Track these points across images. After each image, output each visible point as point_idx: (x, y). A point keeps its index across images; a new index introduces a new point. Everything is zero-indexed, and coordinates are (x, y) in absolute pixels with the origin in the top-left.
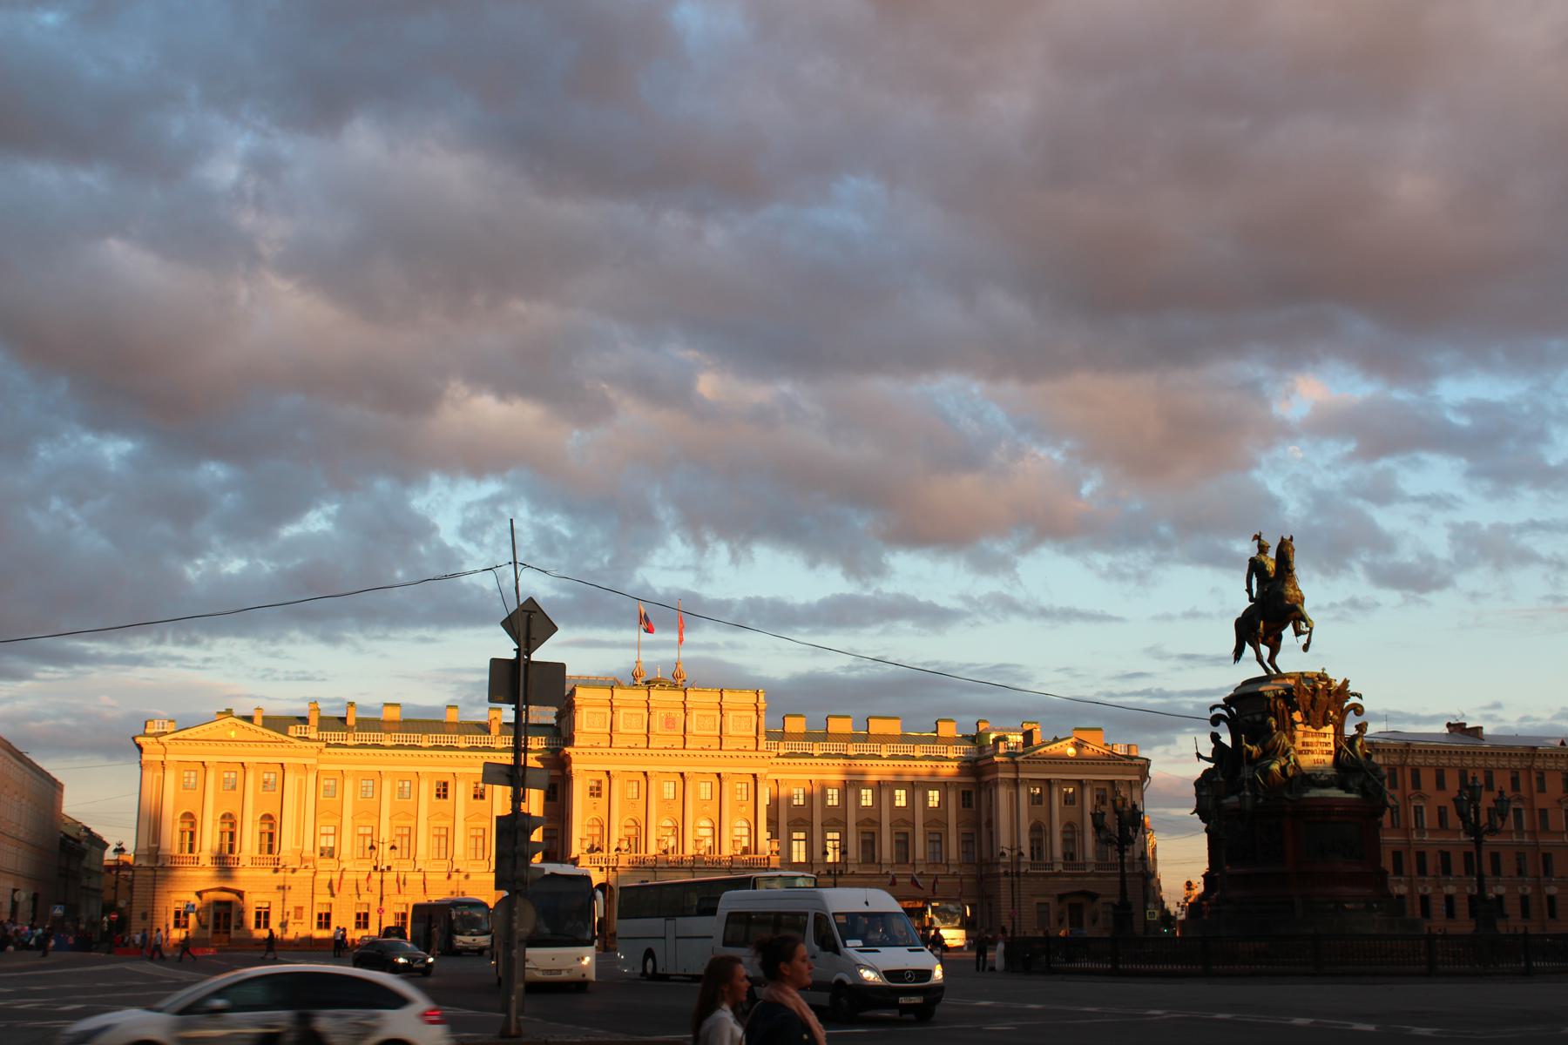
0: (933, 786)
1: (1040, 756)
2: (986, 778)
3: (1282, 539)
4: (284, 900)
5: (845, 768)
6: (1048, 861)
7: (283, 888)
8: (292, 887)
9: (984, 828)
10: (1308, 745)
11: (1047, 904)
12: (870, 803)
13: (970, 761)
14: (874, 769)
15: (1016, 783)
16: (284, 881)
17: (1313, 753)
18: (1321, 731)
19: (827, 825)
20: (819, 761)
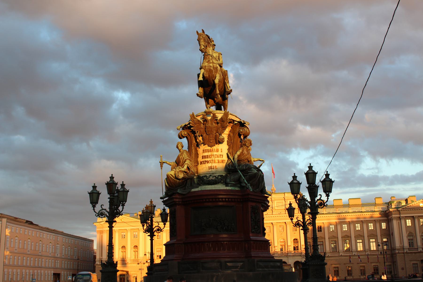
0: (370, 222)
1: (408, 208)
2: (390, 217)
3: (197, 32)
4: (141, 273)
5: (338, 217)
6: (416, 247)
7: (141, 269)
8: (144, 269)
9: (391, 235)
10: (205, 158)
11: (417, 264)
12: (346, 229)
13: (383, 212)
14: (349, 217)
15: (400, 218)
16: (141, 267)
17: (208, 162)
19: (330, 239)
20: (326, 215)
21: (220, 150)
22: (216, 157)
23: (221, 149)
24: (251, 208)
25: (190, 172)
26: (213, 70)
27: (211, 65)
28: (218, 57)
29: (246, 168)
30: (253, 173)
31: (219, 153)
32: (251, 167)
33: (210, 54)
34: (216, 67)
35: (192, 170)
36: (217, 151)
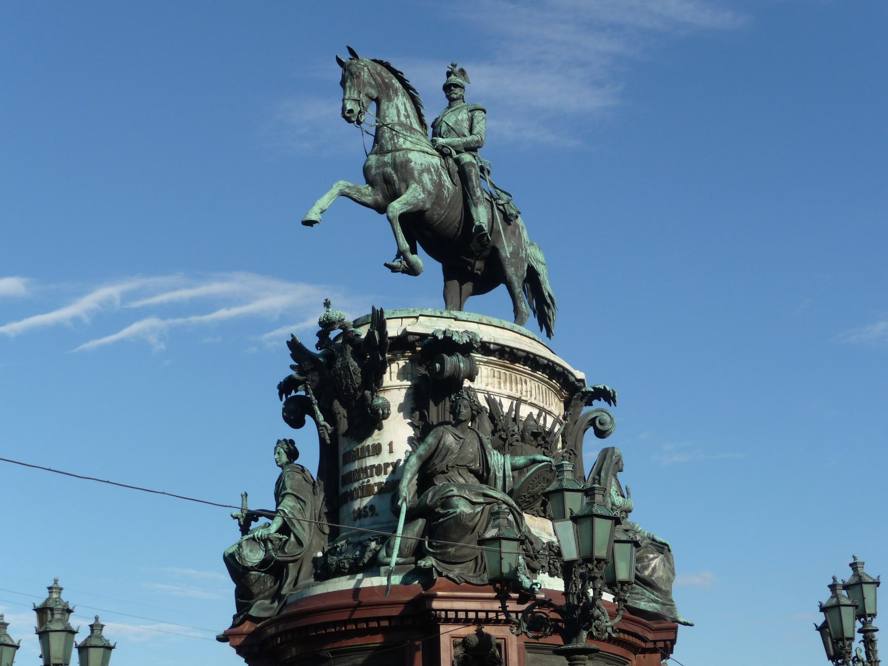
18: (369, 442)
21: (385, 448)
22: (372, 476)
23: (391, 444)
24: (455, 646)
25: (289, 537)
26: (394, 175)
27: (388, 158)
28: (466, 125)
29: (432, 499)
30: (451, 514)
31: (385, 458)
32: (450, 494)
33: (388, 121)
34: (402, 162)
35: (296, 531)
36: (377, 450)
